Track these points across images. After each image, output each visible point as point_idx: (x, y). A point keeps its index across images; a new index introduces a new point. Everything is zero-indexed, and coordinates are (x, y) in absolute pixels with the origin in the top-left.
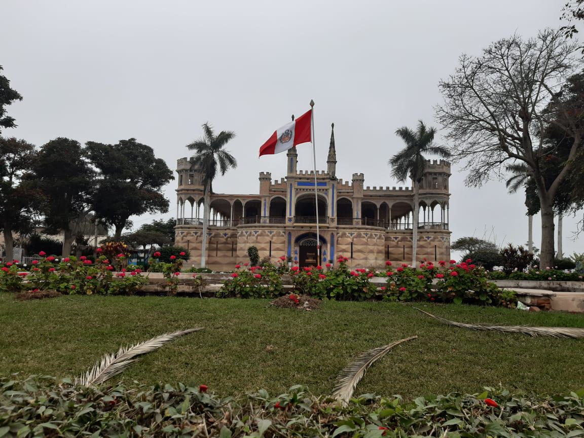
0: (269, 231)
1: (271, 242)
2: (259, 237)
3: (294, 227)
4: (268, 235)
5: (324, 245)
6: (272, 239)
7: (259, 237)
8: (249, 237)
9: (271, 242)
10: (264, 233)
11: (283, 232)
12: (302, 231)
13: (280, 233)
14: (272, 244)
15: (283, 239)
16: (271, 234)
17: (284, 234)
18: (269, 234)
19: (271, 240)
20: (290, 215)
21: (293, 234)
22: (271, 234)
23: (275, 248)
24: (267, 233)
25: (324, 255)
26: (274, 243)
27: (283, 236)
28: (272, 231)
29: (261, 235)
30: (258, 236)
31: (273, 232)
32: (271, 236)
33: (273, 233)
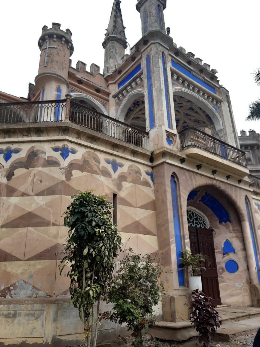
0: (111, 158)
1: (115, 195)
2: (76, 173)
3: (182, 161)
4: (106, 173)
5: (220, 226)
6: (120, 187)
7: (76, 173)
8: (19, 172)
9: (115, 195)
10: (93, 162)
11: (148, 174)
12: (198, 177)
13: (138, 172)
14: (119, 207)
15: (149, 193)
16: (115, 170)
17: (148, 178)
18: (109, 167)
19: (116, 190)
20: (170, 126)
21: (182, 178)
22: (115, 170)
23: (129, 222)
24: (103, 164)
25: (225, 253)
26: (126, 203)
27: (146, 184)
28: (118, 160)
29: (83, 166)
30: (72, 166)
31: (121, 166)
32: (115, 175)
33: (120, 170)
